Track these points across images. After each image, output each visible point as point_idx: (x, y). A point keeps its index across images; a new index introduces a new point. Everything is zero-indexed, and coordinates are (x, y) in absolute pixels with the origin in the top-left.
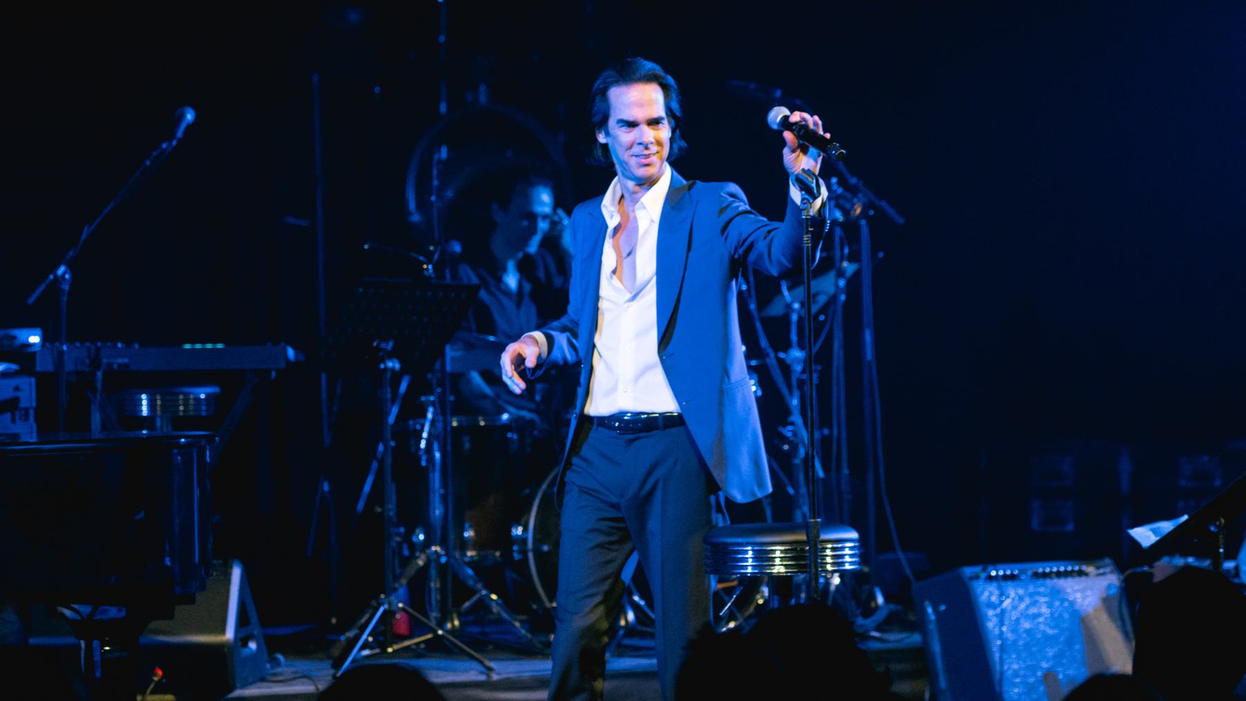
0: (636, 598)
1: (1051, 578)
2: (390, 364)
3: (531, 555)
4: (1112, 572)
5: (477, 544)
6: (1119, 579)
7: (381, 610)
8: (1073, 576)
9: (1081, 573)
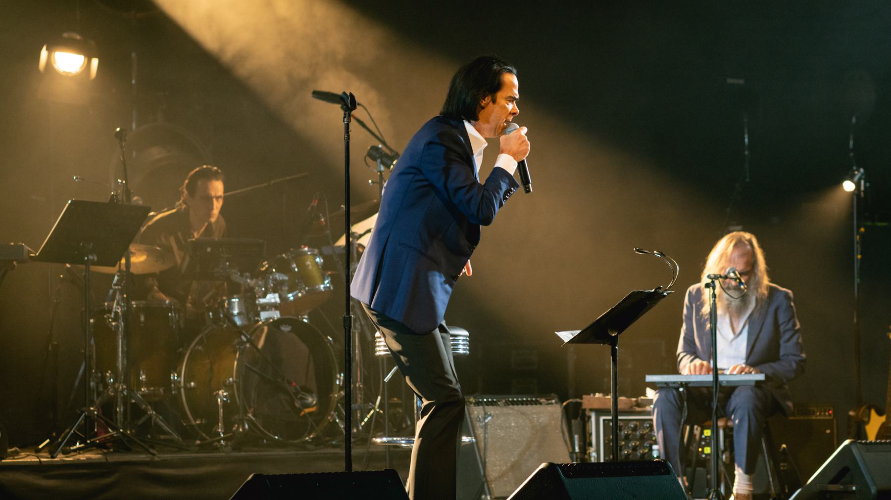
0: (250, 415)
1: (518, 405)
2: (91, 257)
3: (182, 390)
4: (556, 403)
5: (148, 384)
6: (561, 407)
7: (84, 414)
8: (532, 404)
9: (537, 403)
